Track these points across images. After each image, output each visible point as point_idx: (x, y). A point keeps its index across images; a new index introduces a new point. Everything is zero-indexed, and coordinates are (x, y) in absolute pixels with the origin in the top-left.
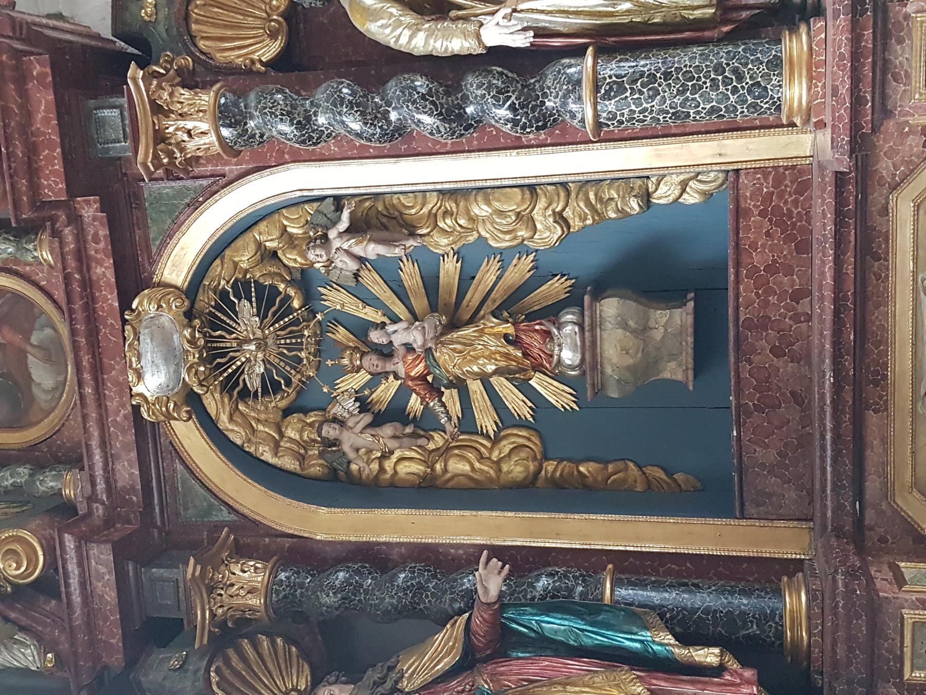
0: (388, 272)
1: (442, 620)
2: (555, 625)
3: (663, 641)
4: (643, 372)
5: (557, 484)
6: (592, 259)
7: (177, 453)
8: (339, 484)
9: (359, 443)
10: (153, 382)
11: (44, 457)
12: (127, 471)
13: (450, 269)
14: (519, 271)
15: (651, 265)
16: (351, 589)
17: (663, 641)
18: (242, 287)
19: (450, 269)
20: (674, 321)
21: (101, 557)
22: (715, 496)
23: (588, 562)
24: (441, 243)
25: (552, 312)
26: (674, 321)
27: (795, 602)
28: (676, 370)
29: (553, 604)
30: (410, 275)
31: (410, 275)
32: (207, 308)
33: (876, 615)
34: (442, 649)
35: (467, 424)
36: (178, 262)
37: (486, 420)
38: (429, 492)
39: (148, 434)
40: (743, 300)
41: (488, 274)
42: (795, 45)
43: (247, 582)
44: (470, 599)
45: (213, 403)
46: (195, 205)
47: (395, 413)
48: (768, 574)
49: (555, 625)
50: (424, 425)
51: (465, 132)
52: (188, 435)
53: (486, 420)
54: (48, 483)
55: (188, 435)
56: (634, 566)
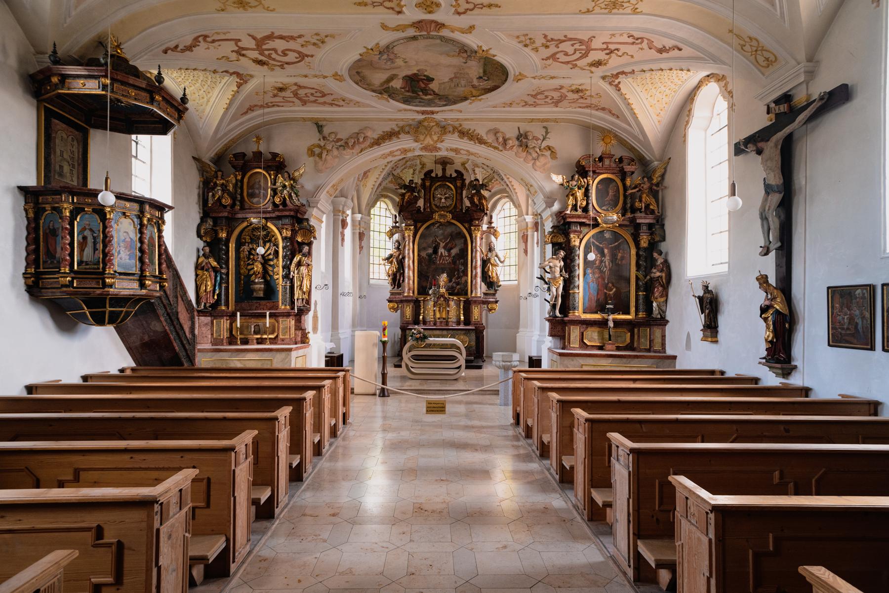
0: (270, 254)
1: (218, 263)
2: (218, 278)
3: (217, 292)
4: (253, 291)
5: (240, 278)
6: (272, 284)
7: (243, 222)
8: (239, 244)
9: (246, 248)
10: (254, 220)
11: (242, 201)
12: (240, 216)
13: (272, 263)
14: (271, 273)
15: (270, 291)
16: (222, 249)
17: (217, 292)
18: (269, 233)
19: (272, 263)
20: (261, 294)
21: (226, 214)
22: (238, 300)
23: (228, 283)
24: (275, 261)
25: (264, 277)
26: (261, 294)
27: (223, 308)
28: (255, 295)
29: (221, 278)
30: (271, 257)
31: (271, 257)
32: (265, 228)
33: (222, 316)
34: (214, 264)
35: (249, 264)
36: (269, 224)
37: (249, 267)
38: (238, 258)
39: (244, 219)
40: (263, 302)
41: (270, 268)
42: (288, 307)
43: (224, 235)
44: (221, 267)
45: (250, 228)
46: (278, 229)
47: (250, 253)
48: (227, 305)
49: (218, 278)
50: (249, 259)
51: (284, 268)
52: (245, 224)
53: (249, 267)
54: (238, 203)
55: (245, 224)
56: (227, 288)
